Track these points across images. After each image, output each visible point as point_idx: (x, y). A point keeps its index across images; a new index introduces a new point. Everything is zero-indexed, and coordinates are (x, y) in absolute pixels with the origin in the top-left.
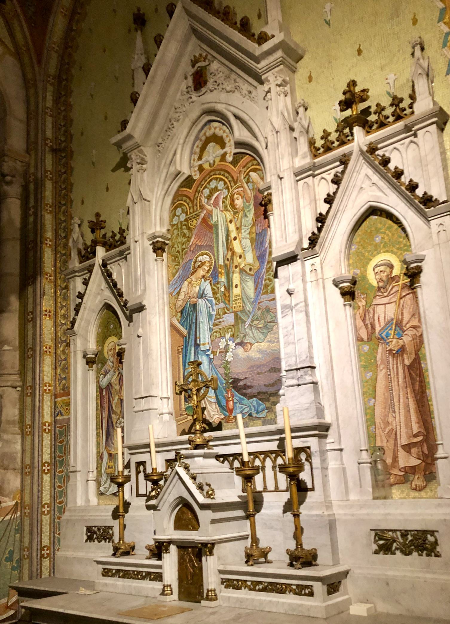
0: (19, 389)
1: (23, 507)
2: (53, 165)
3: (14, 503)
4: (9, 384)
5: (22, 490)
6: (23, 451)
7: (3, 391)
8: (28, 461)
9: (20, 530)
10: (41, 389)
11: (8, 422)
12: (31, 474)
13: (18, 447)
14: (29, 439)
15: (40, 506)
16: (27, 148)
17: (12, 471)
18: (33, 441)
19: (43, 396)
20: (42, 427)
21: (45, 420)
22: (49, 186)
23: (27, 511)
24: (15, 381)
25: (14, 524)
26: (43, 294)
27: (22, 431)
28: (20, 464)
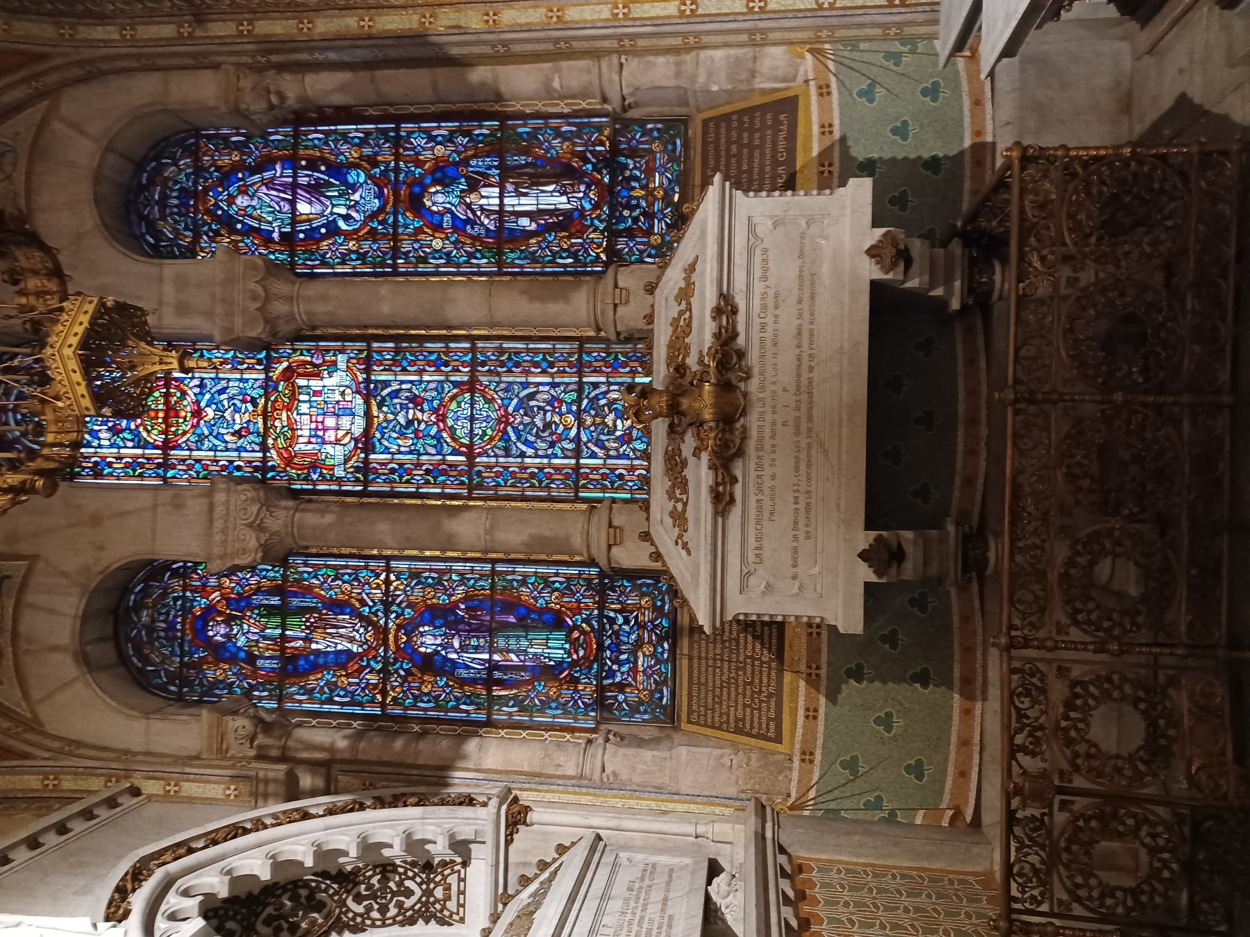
0: (623, 60)
1: (818, 40)
2: (223, 20)
3: (809, 56)
4: (616, 77)
5: (790, 43)
6: (726, 45)
7: (628, 86)
8: (744, 38)
9: (852, 43)
10: (623, 23)
11: (678, 74)
12: (763, 31)
13: (718, 54)
14: (705, 39)
15: (820, 13)
16: (211, 68)
17: (758, 63)
18: (709, 33)
19: (635, 19)
20: (688, 16)
21: (676, 13)
22: (265, 27)
23: (824, 33)
24: (610, 65)
25: (841, 53)
26: (458, 29)
27: (692, 49)
28: (746, 50)
